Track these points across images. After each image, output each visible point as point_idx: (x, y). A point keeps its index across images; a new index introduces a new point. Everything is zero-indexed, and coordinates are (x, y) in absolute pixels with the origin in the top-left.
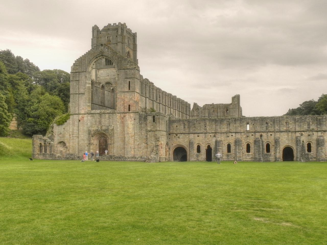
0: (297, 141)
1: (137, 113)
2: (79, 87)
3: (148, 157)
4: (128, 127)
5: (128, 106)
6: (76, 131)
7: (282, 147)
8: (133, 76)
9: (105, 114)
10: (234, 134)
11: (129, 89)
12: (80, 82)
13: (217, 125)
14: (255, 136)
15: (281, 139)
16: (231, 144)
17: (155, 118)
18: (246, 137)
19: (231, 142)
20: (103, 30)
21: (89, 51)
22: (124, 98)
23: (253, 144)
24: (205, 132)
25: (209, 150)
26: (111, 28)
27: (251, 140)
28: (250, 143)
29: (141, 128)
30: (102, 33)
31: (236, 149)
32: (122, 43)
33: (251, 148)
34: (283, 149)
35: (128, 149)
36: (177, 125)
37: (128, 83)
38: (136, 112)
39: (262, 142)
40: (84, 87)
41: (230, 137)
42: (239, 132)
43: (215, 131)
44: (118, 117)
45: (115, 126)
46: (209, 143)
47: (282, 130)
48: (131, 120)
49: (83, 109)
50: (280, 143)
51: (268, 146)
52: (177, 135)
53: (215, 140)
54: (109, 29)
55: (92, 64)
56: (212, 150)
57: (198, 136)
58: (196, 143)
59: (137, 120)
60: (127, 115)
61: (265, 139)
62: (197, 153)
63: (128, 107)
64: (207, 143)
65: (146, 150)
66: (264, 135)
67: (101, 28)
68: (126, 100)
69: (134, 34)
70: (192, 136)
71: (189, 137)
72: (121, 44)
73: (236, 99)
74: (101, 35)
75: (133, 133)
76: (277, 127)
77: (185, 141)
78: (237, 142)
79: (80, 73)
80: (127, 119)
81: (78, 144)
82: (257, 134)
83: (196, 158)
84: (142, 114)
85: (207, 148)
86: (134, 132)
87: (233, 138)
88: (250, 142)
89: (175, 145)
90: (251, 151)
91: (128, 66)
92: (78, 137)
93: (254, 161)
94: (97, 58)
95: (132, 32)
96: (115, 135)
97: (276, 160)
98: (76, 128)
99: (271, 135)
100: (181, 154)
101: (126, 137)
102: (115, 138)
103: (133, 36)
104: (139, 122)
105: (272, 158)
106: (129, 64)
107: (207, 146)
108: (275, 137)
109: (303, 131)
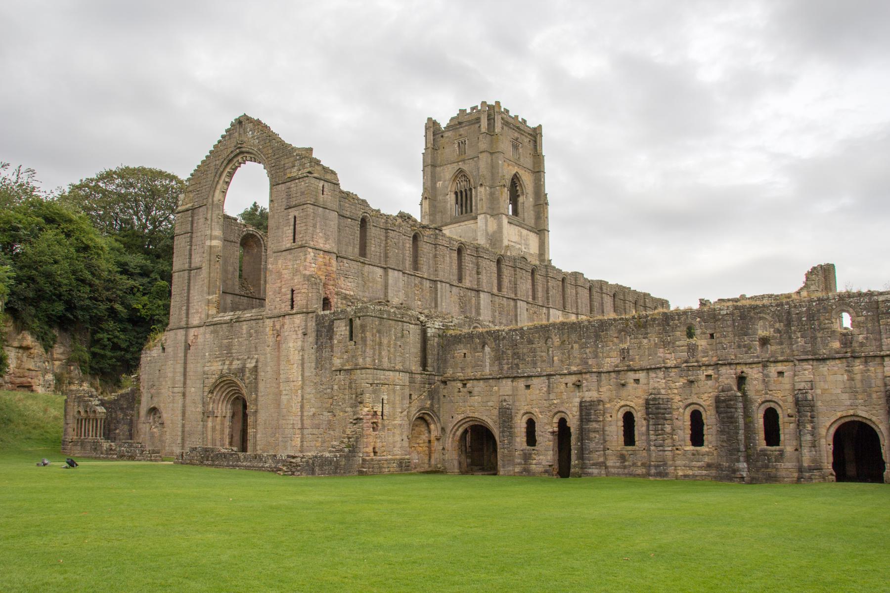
1: (311, 315)
2: (191, 250)
3: (294, 457)
5: (289, 292)
6: (179, 378)
8: (302, 200)
9: (241, 324)
10: (641, 375)
12: (194, 235)
13: (586, 343)
14: (717, 380)
15: (824, 391)
18: (684, 386)
19: (632, 404)
20: (449, 127)
21: (215, 147)
23: (713, 412)
24: (549, 371)
26: (466, 118)
27: (705, 397)
28: (701, 409)
29: (319, 364)
30: (446, 135)
32: (492, 154)
33: (705, 428)
34: (832, 431)
35: (287, 431)
36: (464, 351)
37: (292, 223)
38: (310, 310)
40: (201, 250)
41: (631, 385)
42: (660, 368)
43: (580, 368)
44: (268, 329)
45: (262, 359)
46: (562, 409)
47: (823, 352)
48: (294, 337)
49: (197, 312)
50: (819, 403)
51: (771, 417)
52: (465, 385)
53: (578, 400)
54: (460, 123)
55: (221, 182)
57: (528, 387)
58: (522, 412)
59: (311, 338)
61: (757, 391)
62: (525, 446)
63: (289, 296)
64: (556, 410)
66: (754, 374)
67: (444, 124)
70: (506, 386)
72: (489, 155)
74: (443, 140)
75: (300, 379)
76: (801, 341)
77: (490, 404)
78: (656, 409)
79: (196, 211)
81: (184, 413)
82: (723, 370)
83: (520, 464)
84: (324, 316)
85: (556, 429)
86: (303, 375)
87: (640, 392)
88: (703, 403)
89: (460, 417)
91: (294, 173)
92: (184, 395)
93: (719, 478)
94: (230, 161)
95: (528, 124)
96: (261, 386)
97: (803, 476)
98: (180, 368)
99: (781, 373)
100: (480, 449)
101: (284, 392)
102: (259, 394)
103: (531, 135)
104: (317, 344)
105: (787, 467)
106: (297, 163)
107: (556, 420)
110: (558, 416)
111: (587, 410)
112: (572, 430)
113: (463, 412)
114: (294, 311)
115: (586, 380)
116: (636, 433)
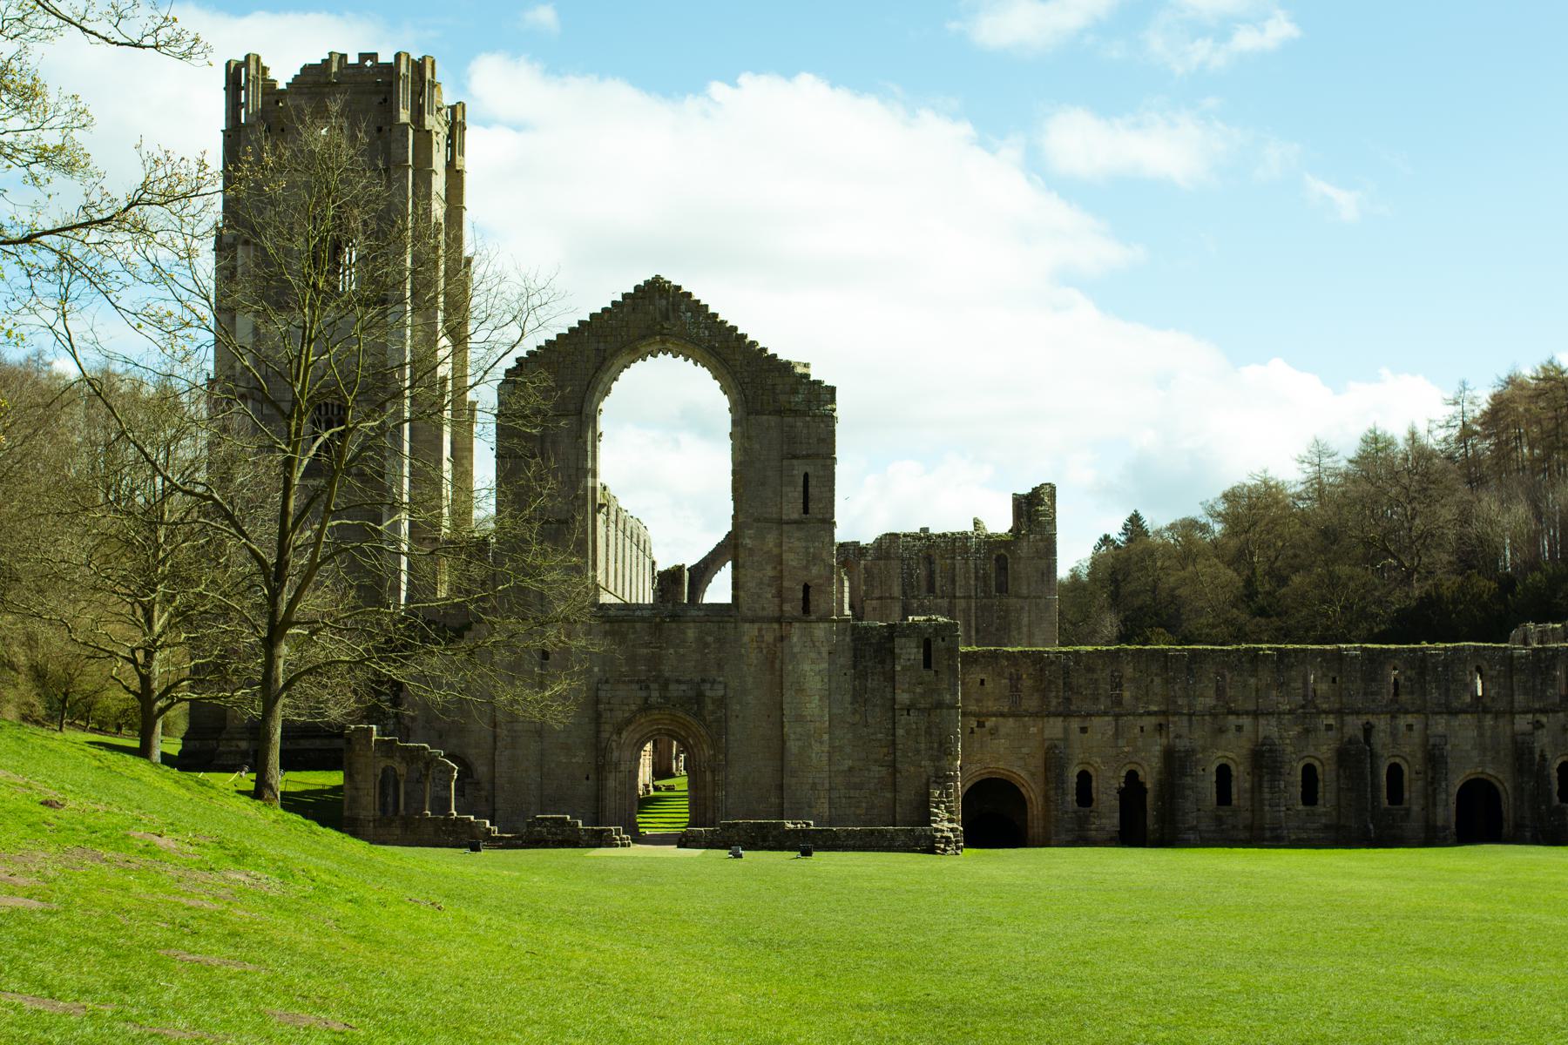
0: (1523, 756)
4: (801, 690)
7: (1456, 782)
10: (1246, 721)
11: (806, 510)
16: (1233, 767)
17: (933, 647)
22: (776, 551)
23: (1334, 767)
25: (1132, 789)
27: (1323, 751)
28: (1317, 764)
29: (859, 696)
31: (1261, 786)
36: (983, 676)
39: (1373, 755)
41: (1231, 734)
43: (1163, 707)
46: (1135, 759)
47: (1455, 704)
48: (813, 655)
52: (981, 725)
56: (1145, 791)
59: (845, 660)
60: (796, 633)
61: (1384, 745)
65: (889, 795)
66: (1381, 723)
67: (283, 74)
68: (791, 560)
69: (453, 108)
71: (1042, 731)
73: (1034, 509)
78: (1264, 760)
80: (796, 650)
82: (1349, 719)
90: (1320, 794)
97: (1431, 837)
99: (1410, 727)
104: (855, 667)
107: (1123, 773)
108: (1427, 738)
109: (1543, 711)
110: (1128, 768)
111: (1175, 763)
112: (1149, 786)
113: (979, 761)
114: (813, 617)
115: (1174, 723)
116: (1234, 790)
